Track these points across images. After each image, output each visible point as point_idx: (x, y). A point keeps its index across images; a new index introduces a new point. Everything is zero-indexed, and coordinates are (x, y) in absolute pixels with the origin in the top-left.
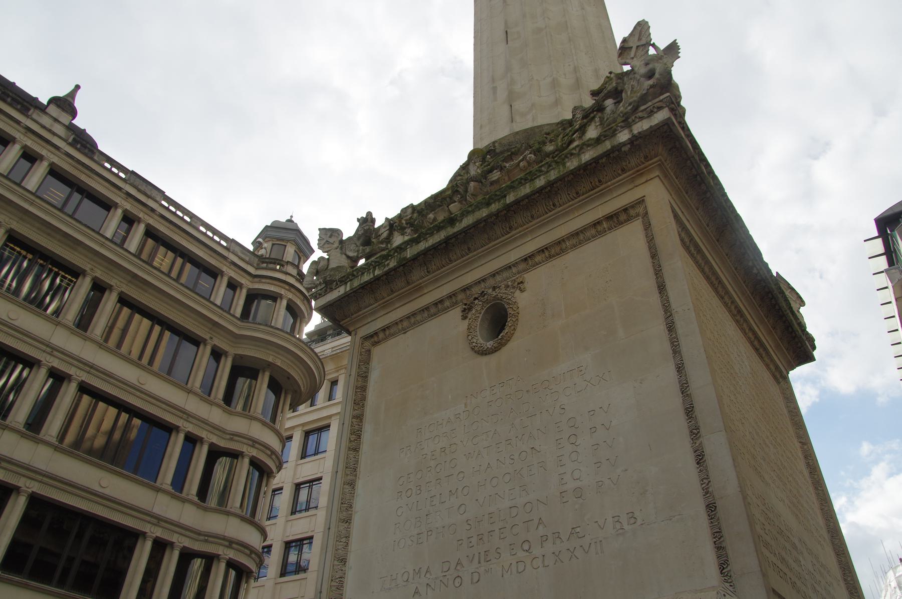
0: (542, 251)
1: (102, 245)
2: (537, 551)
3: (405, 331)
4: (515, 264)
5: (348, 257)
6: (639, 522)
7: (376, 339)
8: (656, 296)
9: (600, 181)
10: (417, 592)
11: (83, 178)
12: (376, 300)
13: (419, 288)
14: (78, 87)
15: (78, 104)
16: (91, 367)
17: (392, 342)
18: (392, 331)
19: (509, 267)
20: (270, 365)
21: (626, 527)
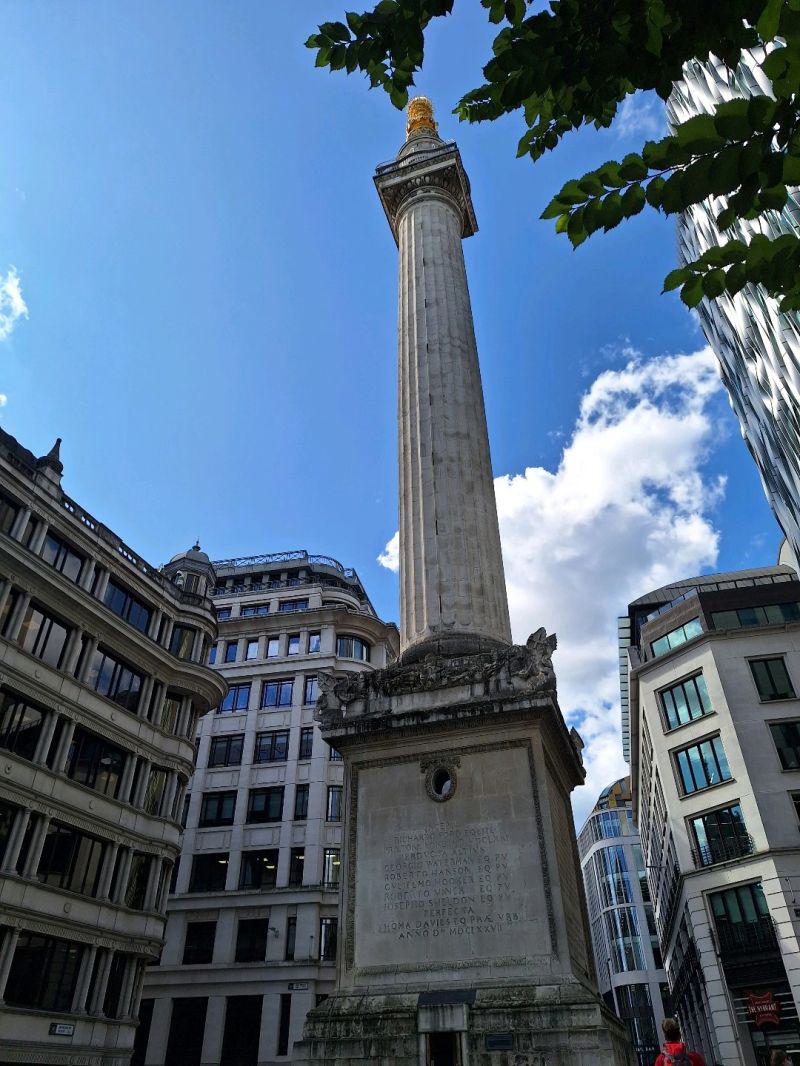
1: (96, 607)
2: (469, 925)
5: (340, 700)
8: (532, 800)
10: (402, 936)
11: (71, 536)
12: (365, 742)
14: (59, 441)
15: (62, 459)
16: (85, 712)
20: (193, 693)
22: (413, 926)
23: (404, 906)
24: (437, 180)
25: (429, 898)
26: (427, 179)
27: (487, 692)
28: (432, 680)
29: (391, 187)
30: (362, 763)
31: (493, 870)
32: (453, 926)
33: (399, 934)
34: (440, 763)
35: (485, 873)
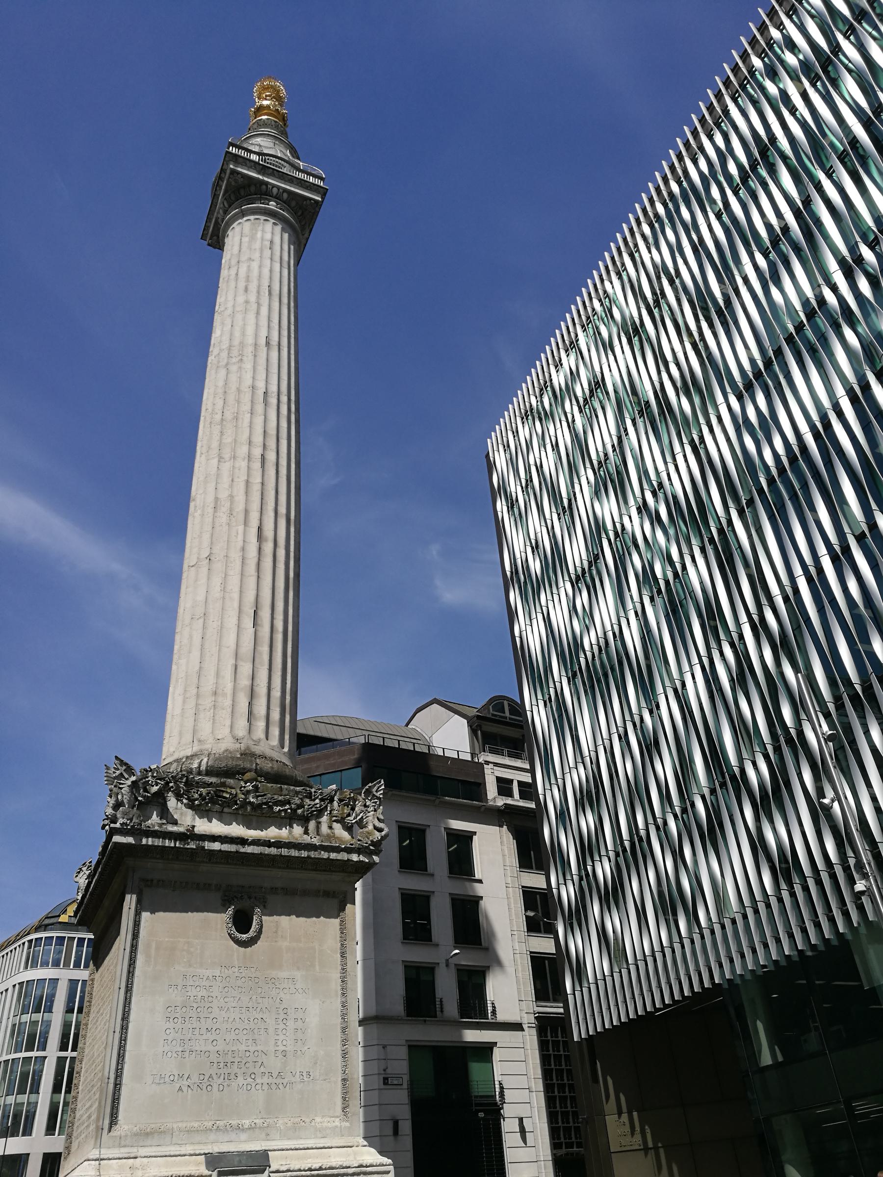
2: (259, 1081)
10: (180, 1089)
22: (195, 1078)
23: (187, 1054)
24: (293, 204)
25: (217, 1048)
27: (306, 832)
29: (244, 176)
31: (291, 1024)
32: (240, 1080)
35: (282, 1026)
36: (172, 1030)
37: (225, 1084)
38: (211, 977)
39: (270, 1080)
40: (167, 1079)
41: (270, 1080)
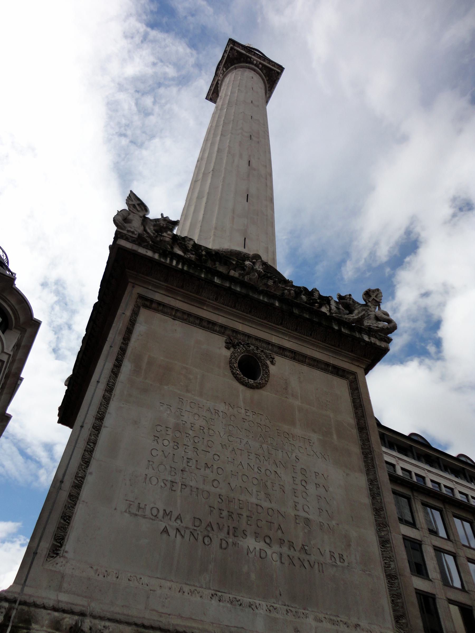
0: (291, 351)
3: (175, 318)
4: (273, 345)
6: (346, 564)
7: (148, 303)
9: (339, 346)
10: (165, 531)
13: (201, 303)
17: (159, 316)
18: (165, 310)
19: (268, 343)
21: (339, 563)
22: (187, 521)
26: (260, 66)
28: (259, 273)
30: (152, 301)
31: (311, 488)
33: (162, 525)
34: (252, 347)
35: (300, 488)
36: (160, 453)
37: (230, 540)
38: (212, 410)
39: (292, 553)
40: (148, 512)
41: (292, 553)
